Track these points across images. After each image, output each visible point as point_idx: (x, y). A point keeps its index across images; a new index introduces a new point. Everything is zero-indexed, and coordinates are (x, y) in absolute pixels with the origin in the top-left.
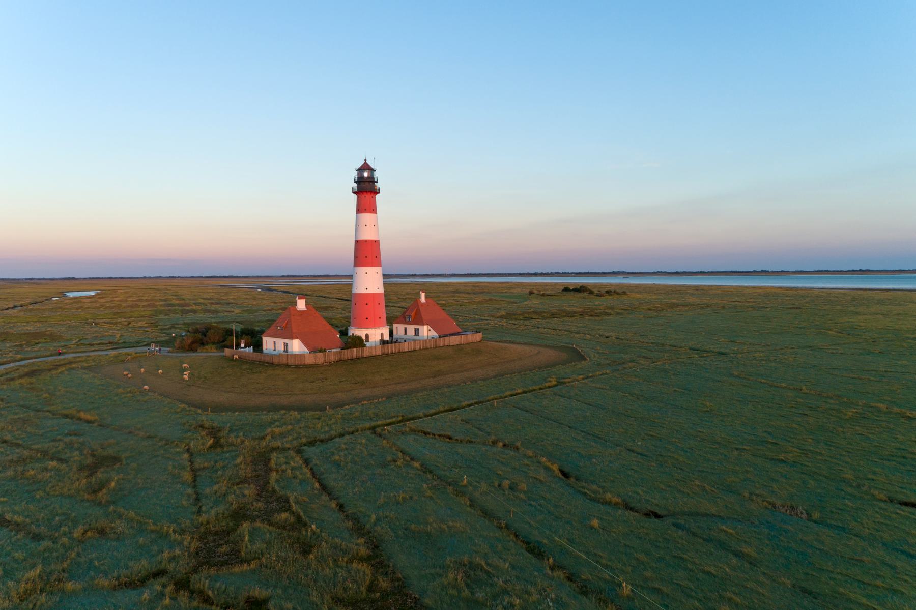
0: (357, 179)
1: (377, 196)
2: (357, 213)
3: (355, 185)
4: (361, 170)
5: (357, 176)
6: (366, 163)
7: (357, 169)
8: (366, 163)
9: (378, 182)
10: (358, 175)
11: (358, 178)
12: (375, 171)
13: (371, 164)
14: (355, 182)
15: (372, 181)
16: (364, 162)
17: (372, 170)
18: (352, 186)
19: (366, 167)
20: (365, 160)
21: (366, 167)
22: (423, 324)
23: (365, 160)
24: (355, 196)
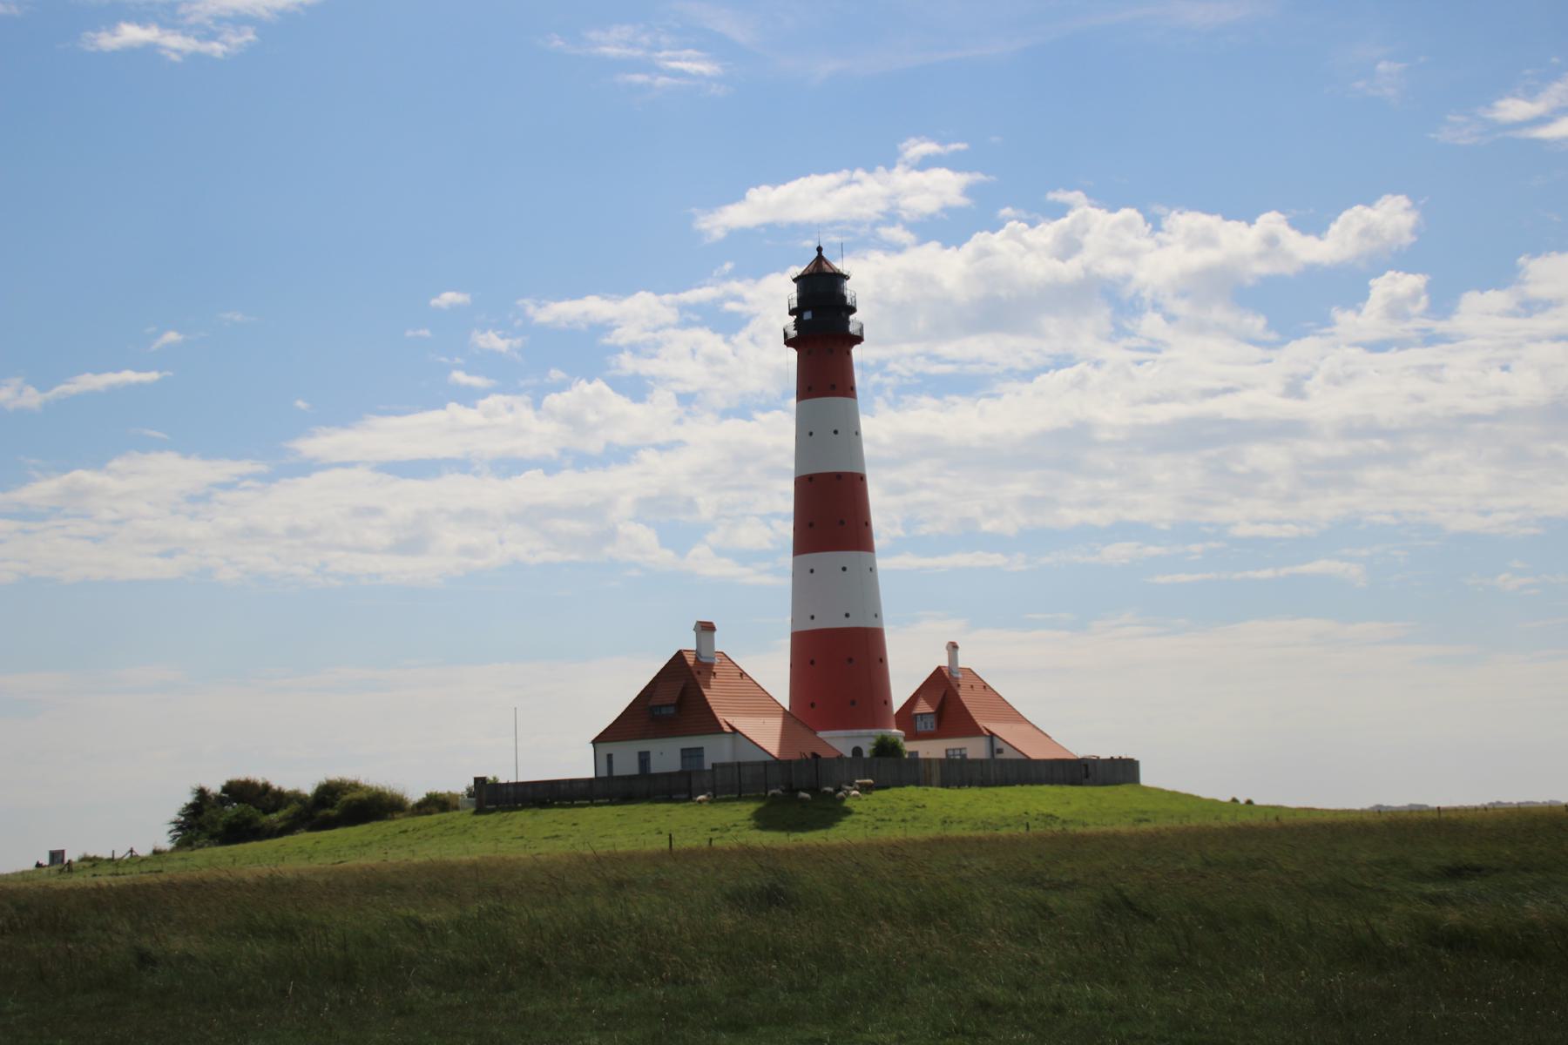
1: (856, 351)
2: (798, 400)
5: (795, 295)
6: (820, 258)
7: (794, 277)
8: (820, 258)
9: (858, 308)
10: (800, 290)
11: (799, 300)
12: (848, 278)
14: (792, 313)
16: (816, 254)
20: (819, 249)
23: (819, 249)
24: (792, 354)
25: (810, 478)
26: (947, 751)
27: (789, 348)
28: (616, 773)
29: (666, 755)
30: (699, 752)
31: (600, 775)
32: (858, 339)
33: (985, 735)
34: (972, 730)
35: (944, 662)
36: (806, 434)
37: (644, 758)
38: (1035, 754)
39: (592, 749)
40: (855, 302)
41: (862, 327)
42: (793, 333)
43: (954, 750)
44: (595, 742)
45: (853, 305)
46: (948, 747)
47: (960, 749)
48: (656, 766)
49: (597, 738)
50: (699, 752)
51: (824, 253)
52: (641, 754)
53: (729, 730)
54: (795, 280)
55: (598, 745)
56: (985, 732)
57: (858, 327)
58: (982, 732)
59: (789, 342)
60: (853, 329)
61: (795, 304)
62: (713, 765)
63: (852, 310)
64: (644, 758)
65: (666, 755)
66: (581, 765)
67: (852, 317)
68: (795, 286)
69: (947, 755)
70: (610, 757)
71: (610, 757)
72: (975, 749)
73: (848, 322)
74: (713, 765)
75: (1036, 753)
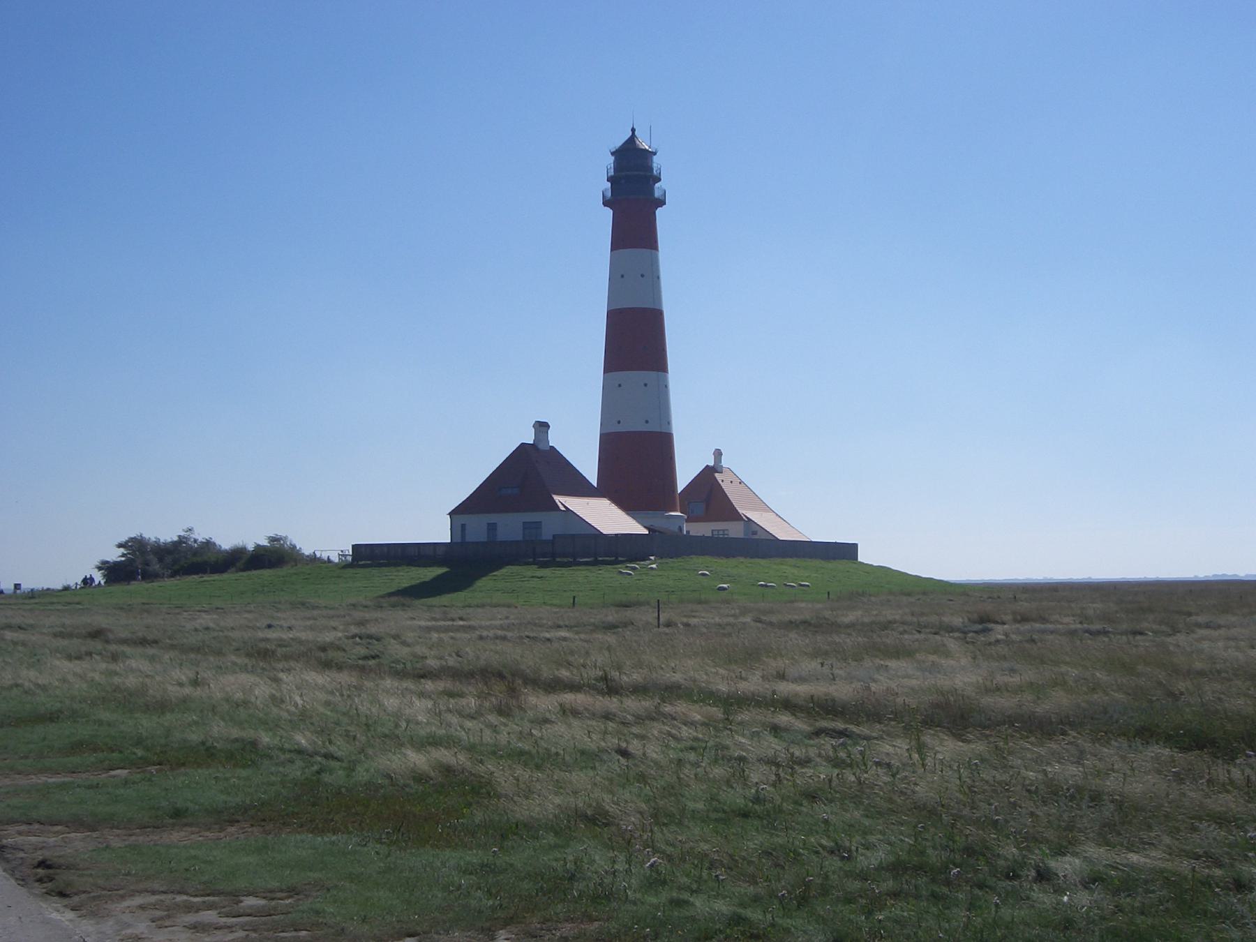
0: (612, 170)
1: (659, 211)
3: (609, 185)
5: (612, 165)
6: (632, 139)
8: (633, 136)
9: (662, 178)
11: (615, 169)
12: (655, 154)
20: (633, 130)
23: (633, 130)
24: (609, 213)
26: (713, 531)
27: (606, 208)
28: (468, 539)
29: (510, 526)
30: (538, 525)
31: (454, 541)
32: (661, 203)
33: (744, 520)
34: (734, 515)
35: (711, 463)
36: (617, 277)
37: (492, 527)
38: (782, 536)
39: (449, 518)
40: (660, 173)
41: (665, 192)
42: (609, 194)
43: (718, 530)
45: (658, 175)
46: (713, 528)
47: (724, 530)
48: (503, 534)
49: (453, 510)
50: (538, 525)
51: (636, 133)
52: (489, 524)
53: (563, 509)
54: (613, 154)
55: (453, 516)
56: (744, 517)
57: (661, 193)
58: (742, 517)
59: (606, 203)
60: (657, 194)
61: (612, 173)
62: (554, 536)
64: (492, 527)
65: (510, 526)
66: (440, 532)
67: (657, 185)
69: (713, 535)
70: (463, 526)
71: (463, 526)
72: (734, 530)
73: (653, 189)
74: (554, 536)
75: (782, 535)
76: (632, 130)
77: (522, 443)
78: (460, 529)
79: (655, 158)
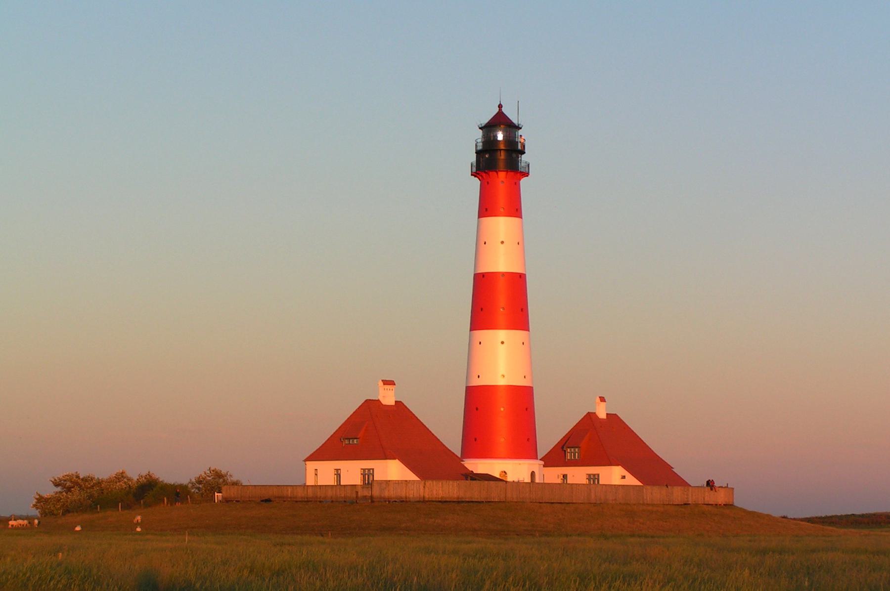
1: (524, 182)
4: (489, 128)
5: (479, 140)
7: (480, 126)
9: (526, 150)
10: (484, 136)
13: (510, 113)
15: (514, 150)
16: (497, 110)
17: (511, 127)
18: (472, 161)
19: (500, 120)
20: (500, 106)
21: (500, 120)
22: (610, 464)
23: (500, 106)
24: (476, 182)
25: (483, 275)
28: (321, 483)
44: (306, 460)
51: (503, 109)
54: (480, 128)
63: (523, 152)
68: (480, 133)
76: (499, 107)
77: (366, 401)
78: (313, 472)
79: (520, 132)
